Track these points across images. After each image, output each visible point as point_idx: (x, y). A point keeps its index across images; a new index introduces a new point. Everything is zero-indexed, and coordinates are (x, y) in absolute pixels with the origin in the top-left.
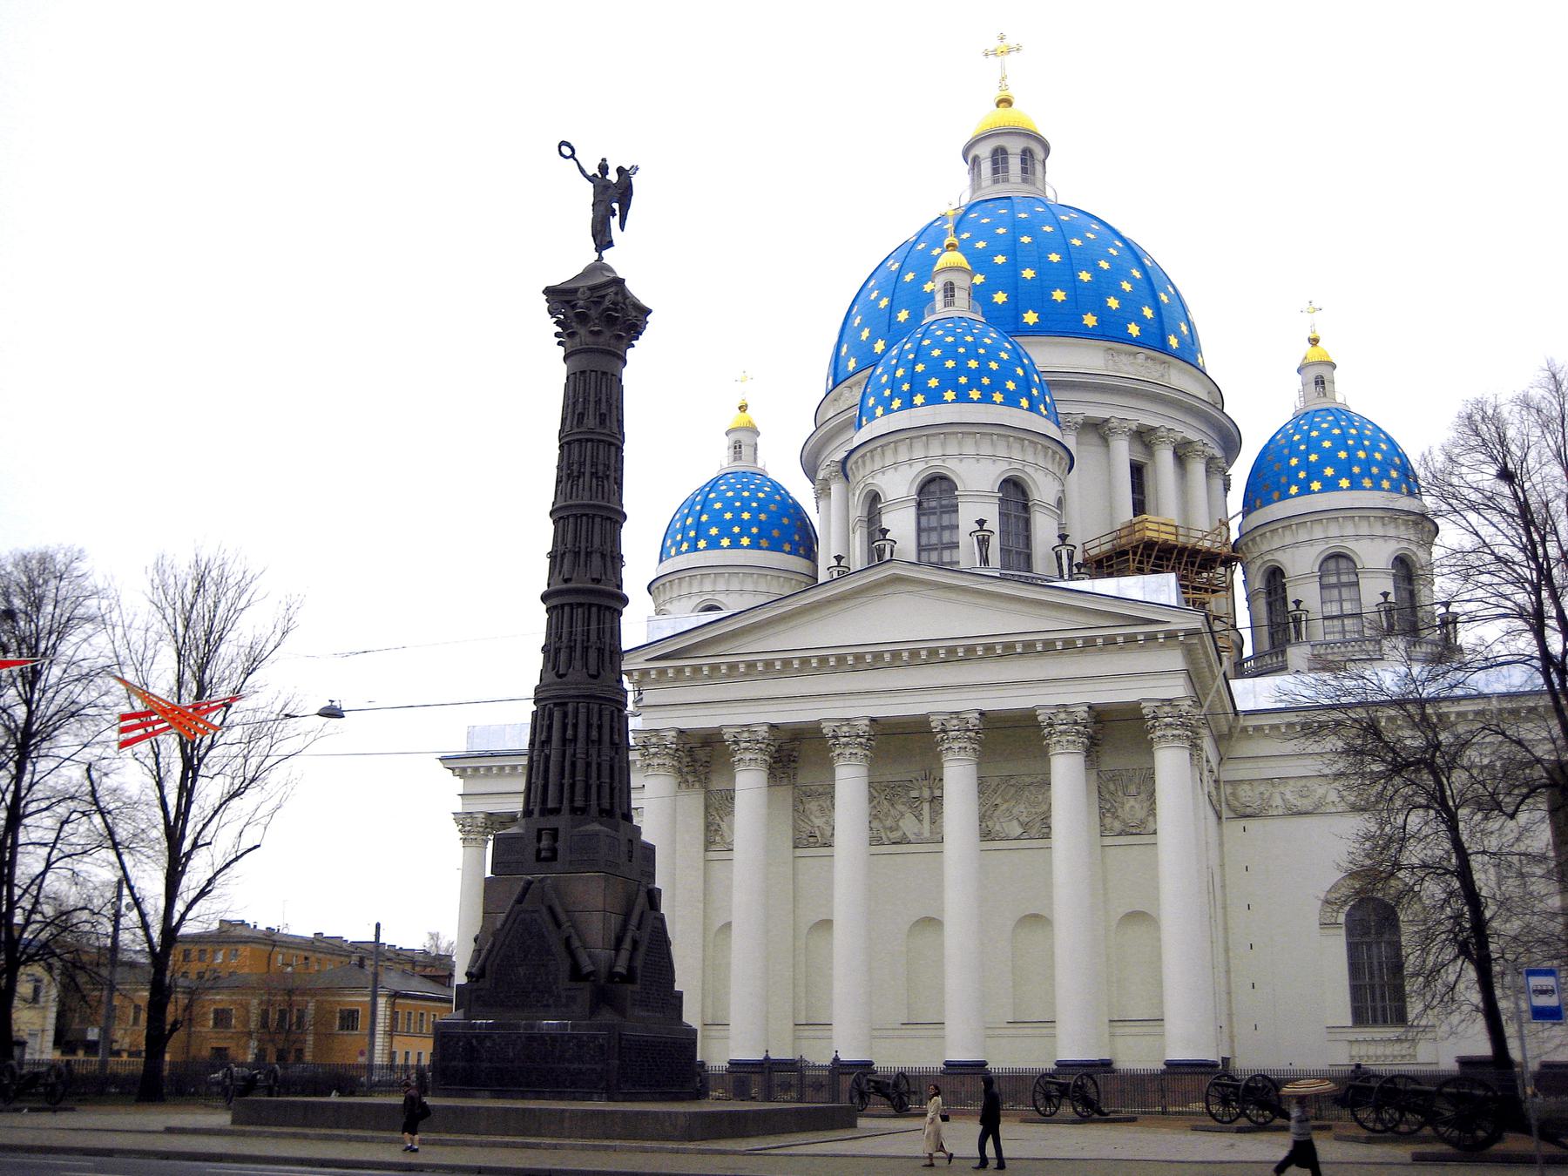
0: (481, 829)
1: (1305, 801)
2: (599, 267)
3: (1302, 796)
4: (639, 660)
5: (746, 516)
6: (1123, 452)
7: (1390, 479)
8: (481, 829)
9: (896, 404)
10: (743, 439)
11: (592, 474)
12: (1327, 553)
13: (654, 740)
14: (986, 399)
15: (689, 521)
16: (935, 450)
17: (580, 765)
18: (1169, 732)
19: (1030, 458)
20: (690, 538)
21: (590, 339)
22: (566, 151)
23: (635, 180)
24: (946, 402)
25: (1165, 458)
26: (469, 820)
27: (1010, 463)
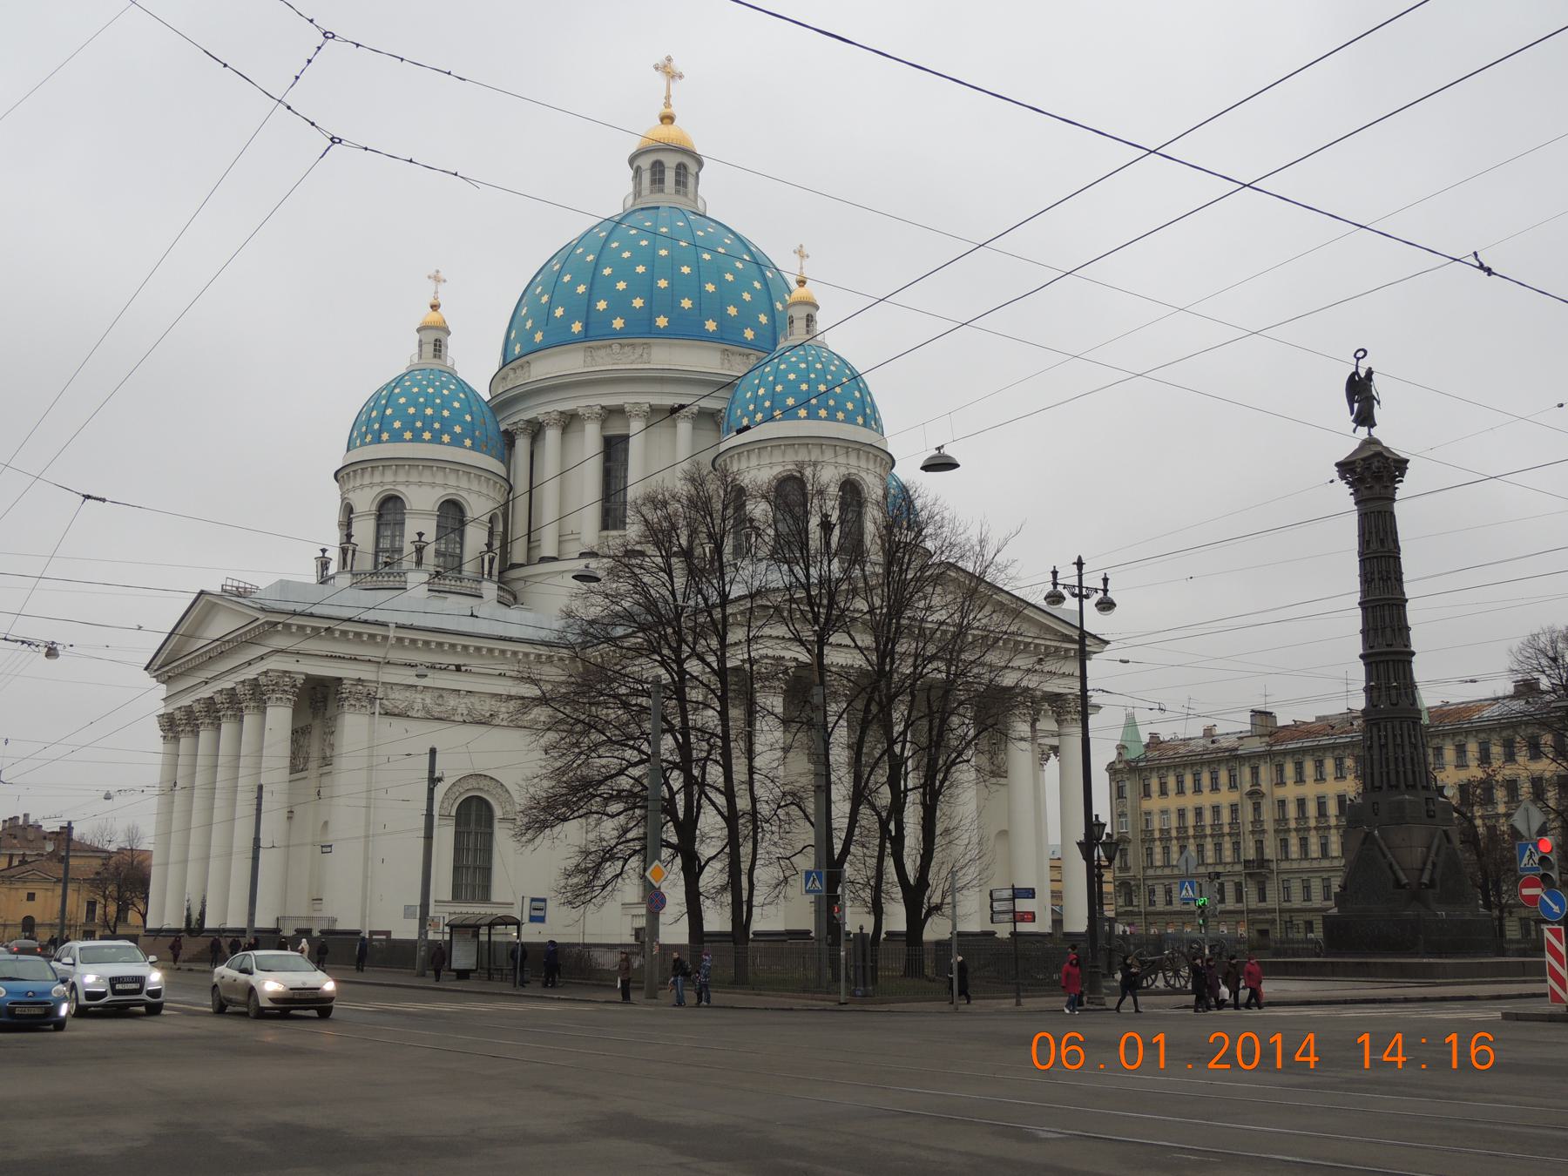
2: (1371, 442)
17: (1392, 759)
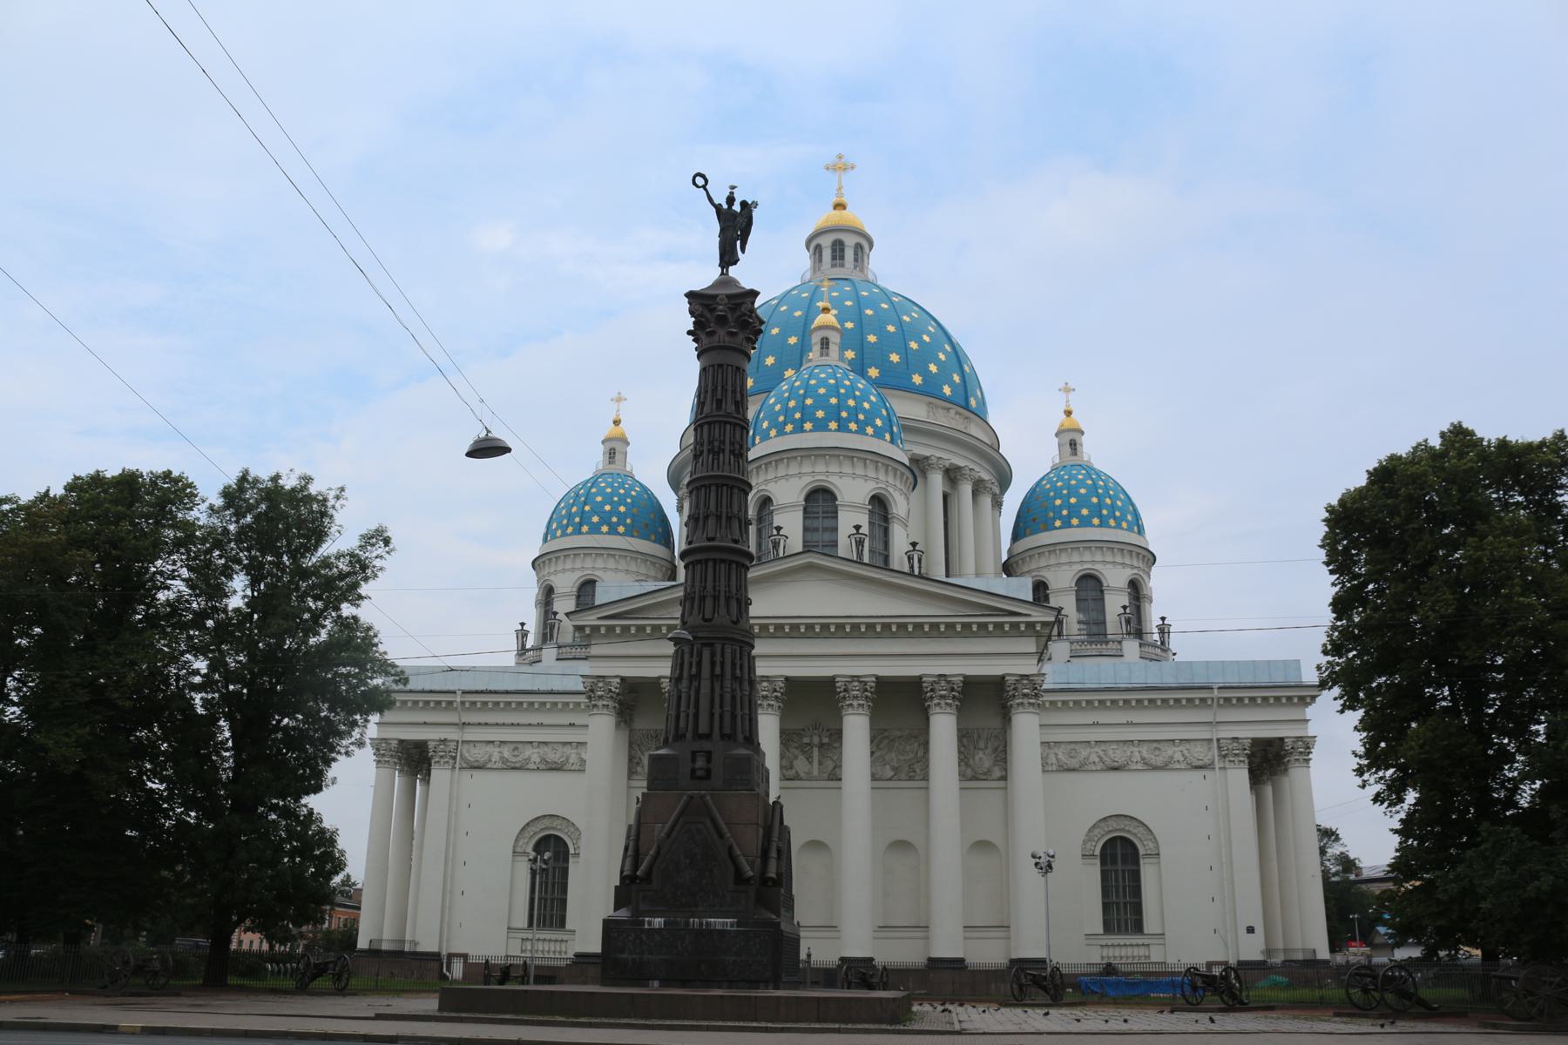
0: (394, 753)
1: (1074, 761)
3: (1071, 757)
4: (594, 617)
5: (622, 509)
6: (937, 481)
7: (1127, 521)
8: (394, 753)
9: (789, 428)
10: (615, 448)
11: (730, 451)
12: (1081, 574)
13: (601, 685)
14: (861, 431)
15: (574, 509)
16: (820, 467)
18: (1026, 701)
19: (891, 480)
20: (575, 523)
21: (727, 339)
22: (700, 181)
23: (756, 214)
24: (830, 430)
25: (966, 489)
26: (383, 745)
27: (877, 483)
